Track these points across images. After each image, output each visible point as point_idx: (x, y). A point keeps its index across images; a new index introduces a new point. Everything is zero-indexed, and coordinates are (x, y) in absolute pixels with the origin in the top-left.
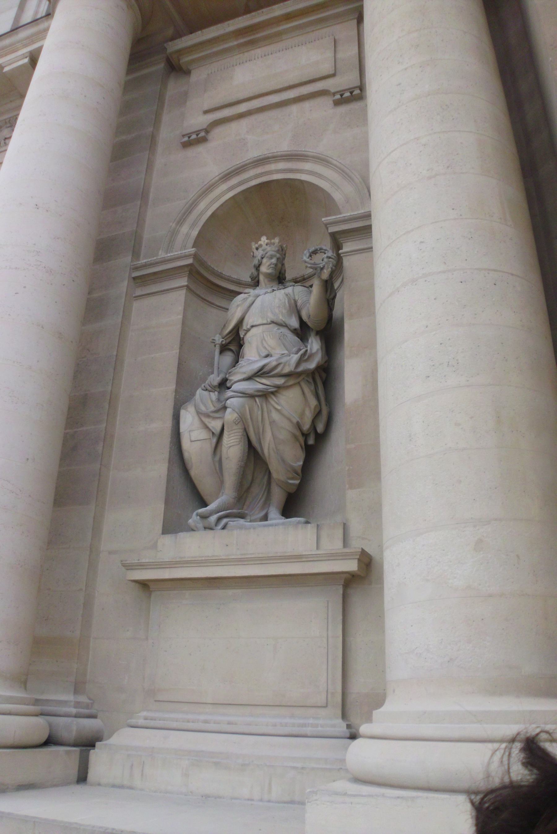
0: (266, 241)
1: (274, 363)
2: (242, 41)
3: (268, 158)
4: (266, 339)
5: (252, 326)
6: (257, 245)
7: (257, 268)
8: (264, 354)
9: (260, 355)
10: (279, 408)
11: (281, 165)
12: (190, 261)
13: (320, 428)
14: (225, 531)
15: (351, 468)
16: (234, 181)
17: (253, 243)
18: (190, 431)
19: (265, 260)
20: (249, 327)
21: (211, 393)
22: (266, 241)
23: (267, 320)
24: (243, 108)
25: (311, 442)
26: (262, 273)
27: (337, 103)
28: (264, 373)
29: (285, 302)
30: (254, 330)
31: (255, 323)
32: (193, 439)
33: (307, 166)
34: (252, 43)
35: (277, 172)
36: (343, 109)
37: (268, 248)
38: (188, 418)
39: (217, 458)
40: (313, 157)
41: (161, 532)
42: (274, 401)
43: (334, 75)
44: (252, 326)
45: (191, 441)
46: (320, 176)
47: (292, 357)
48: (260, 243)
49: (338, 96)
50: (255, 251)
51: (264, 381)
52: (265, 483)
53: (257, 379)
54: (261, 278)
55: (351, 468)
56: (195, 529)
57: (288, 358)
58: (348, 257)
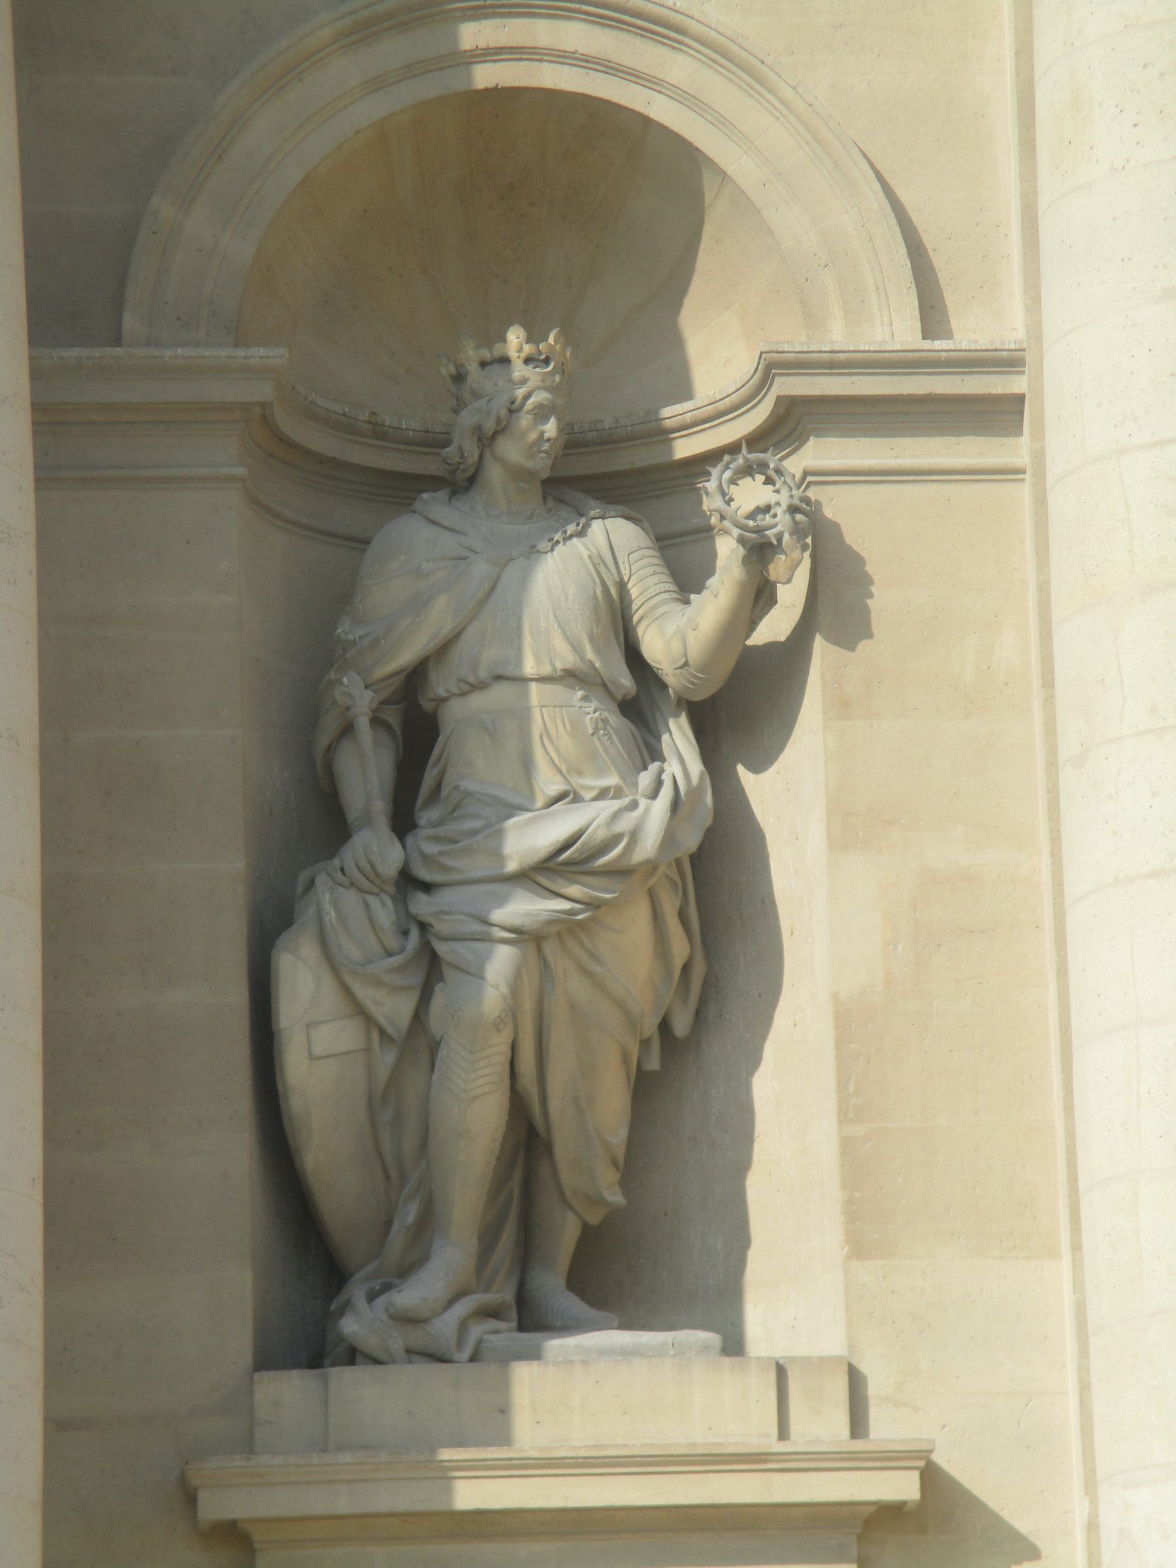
0: (528, 349)
4: (553, 733)
6: (486, 354)
10: (597, 969)
12: (264, 392)
13: (681, 1026)
14: (475, 1364)
15: (857, 1194)
18: (308, 1026)
20: (483, 674)
21: (371, 899)
22: (528, 349)
23: (553, 665)
25: (653, 1063)
26: (501, 461)
28: (569, 863)
29: (595, 592)
32: (318, 1050)
33: (678, 67)
37: (533, 374)
38: (300, 979)
39: (387, 1115)
41: (246, 1357)
42: (582, 945)
44: (499, 678)
45: (312, 1058)
46: (722, 123)
47: (647, 811)
52: (516, 1192)
54: (494, 474)
55: (857, 1194)
57: (636, 814)
58: (831, 488)
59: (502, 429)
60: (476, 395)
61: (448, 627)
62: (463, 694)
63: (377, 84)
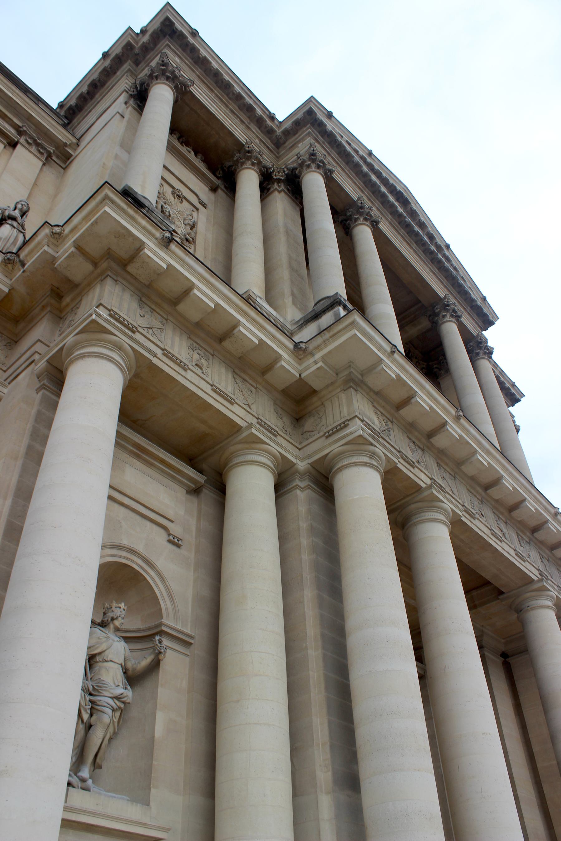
1: (125, 695)
2: (135, 450)
3: (136, 552)
5: (111, 661)
7: (113, 619)
8: (117, 684)
9: (114, 683)
11: (140, 562)
16: (115, 552)
17: (114, 602)
19: (120, 619)
20: (109, 659)
24: (126, 501)
26: (114, 624)
27: (169, 541)
30: (110, 664)
31: (114, 660)
34: (138, 457)
35: (137, 564)
36: (170, 546)
40: (157, 571)
43: (172, 522)
44: (111, 661)
48: (120, 605)
49: (171, 538)
50: (114, 607)
51: (117, 702)
53: (115, 700)
54: (112, 626)
56: (76, 787)
59: (117, 618)
60: (113, 611)
61: (105, 649)
62: (103, 662)
63: (112, 556)
